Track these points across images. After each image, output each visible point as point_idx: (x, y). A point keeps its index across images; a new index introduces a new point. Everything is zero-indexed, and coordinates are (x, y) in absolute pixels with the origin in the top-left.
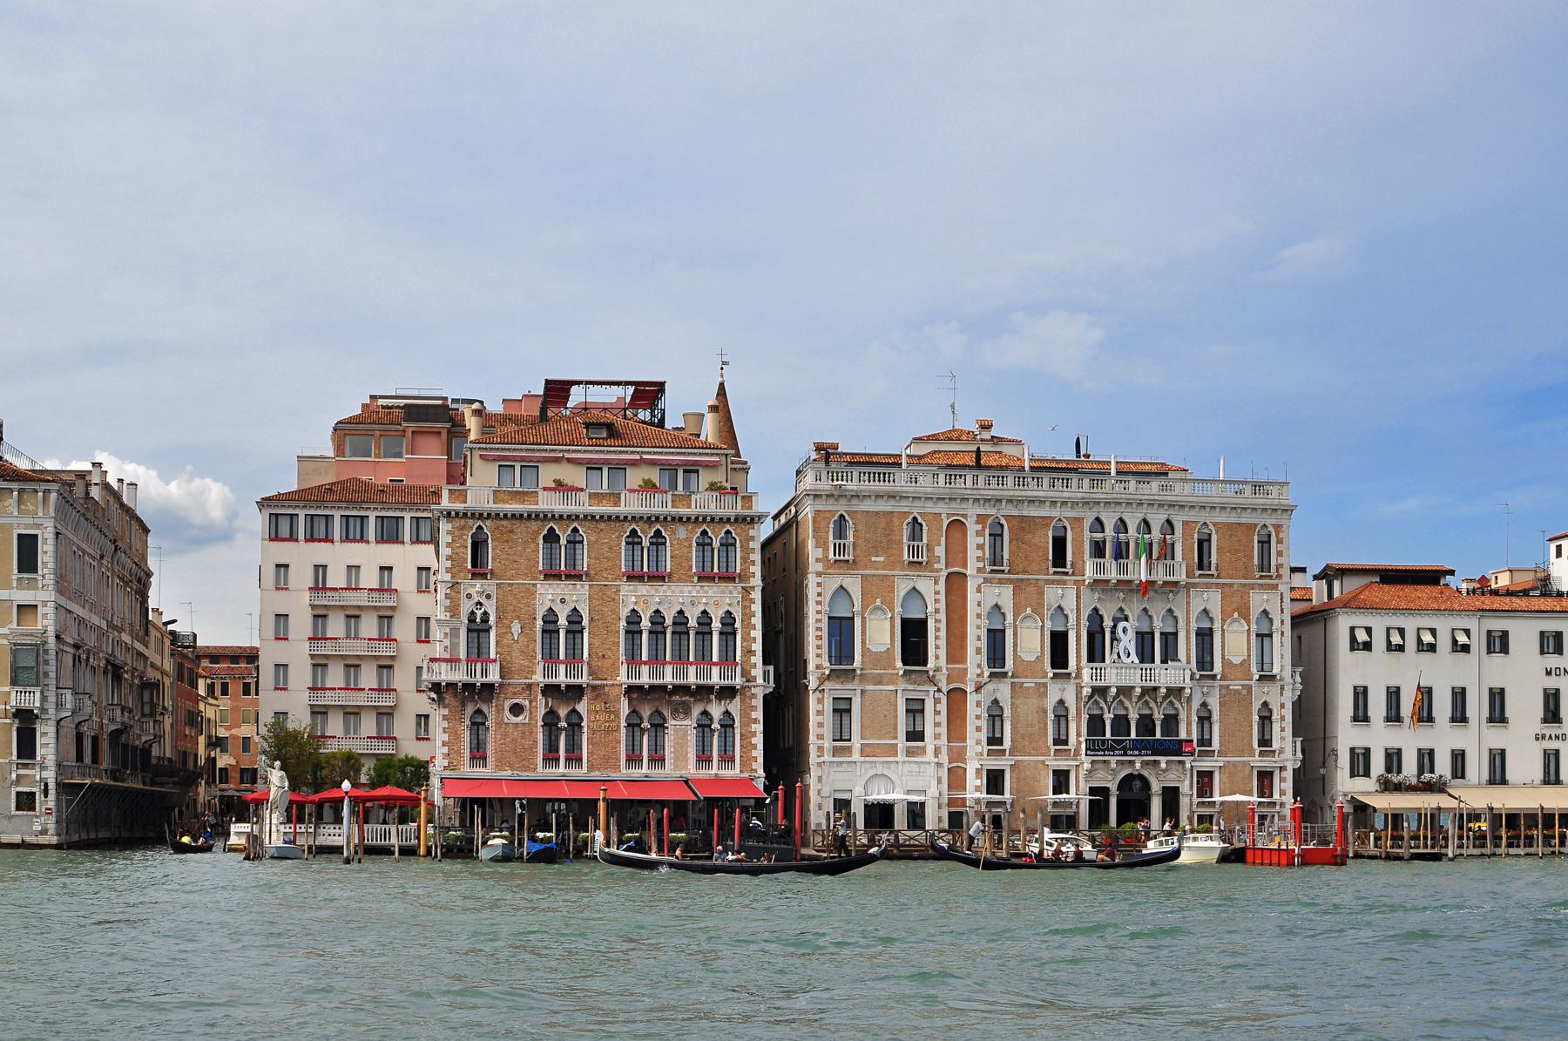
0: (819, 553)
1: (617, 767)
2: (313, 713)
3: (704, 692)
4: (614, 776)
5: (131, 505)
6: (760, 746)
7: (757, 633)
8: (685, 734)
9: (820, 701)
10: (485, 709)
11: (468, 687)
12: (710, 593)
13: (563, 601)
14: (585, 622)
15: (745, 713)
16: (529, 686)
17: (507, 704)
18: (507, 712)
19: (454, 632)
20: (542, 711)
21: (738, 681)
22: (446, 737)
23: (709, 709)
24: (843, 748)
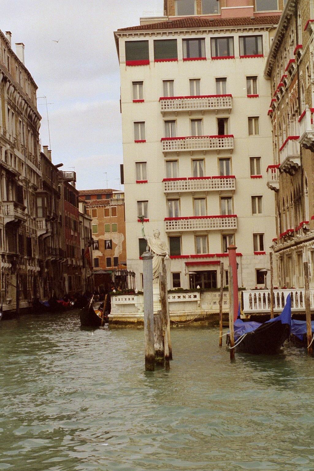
2: (169, 200)
5: (22, 61)
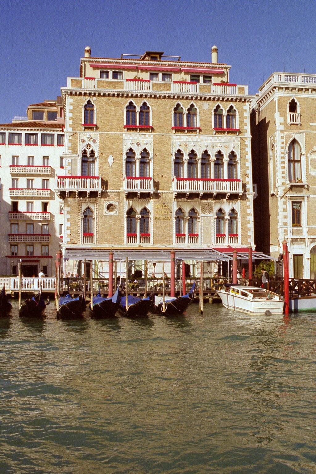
0: (282, 120)
1: (170, 242)
3: (220, 196)
4: (169, 246)
6: (252, 229)
7: (249, 164)
8: (210, 222)
9: (285, 203)
10: (92, 207)
11: (82, 194)
12: (223, 141)
13: (138, 144)
14: (151, 156)
15: (244, 210)
16: (119, 194)
17: (106, 205)
18: (105, 209)
19: (74, 162)
20: (126, 209)
21: (240, 191)
22: (69, 224)
23: (223, 207)
24: (298, 230)
